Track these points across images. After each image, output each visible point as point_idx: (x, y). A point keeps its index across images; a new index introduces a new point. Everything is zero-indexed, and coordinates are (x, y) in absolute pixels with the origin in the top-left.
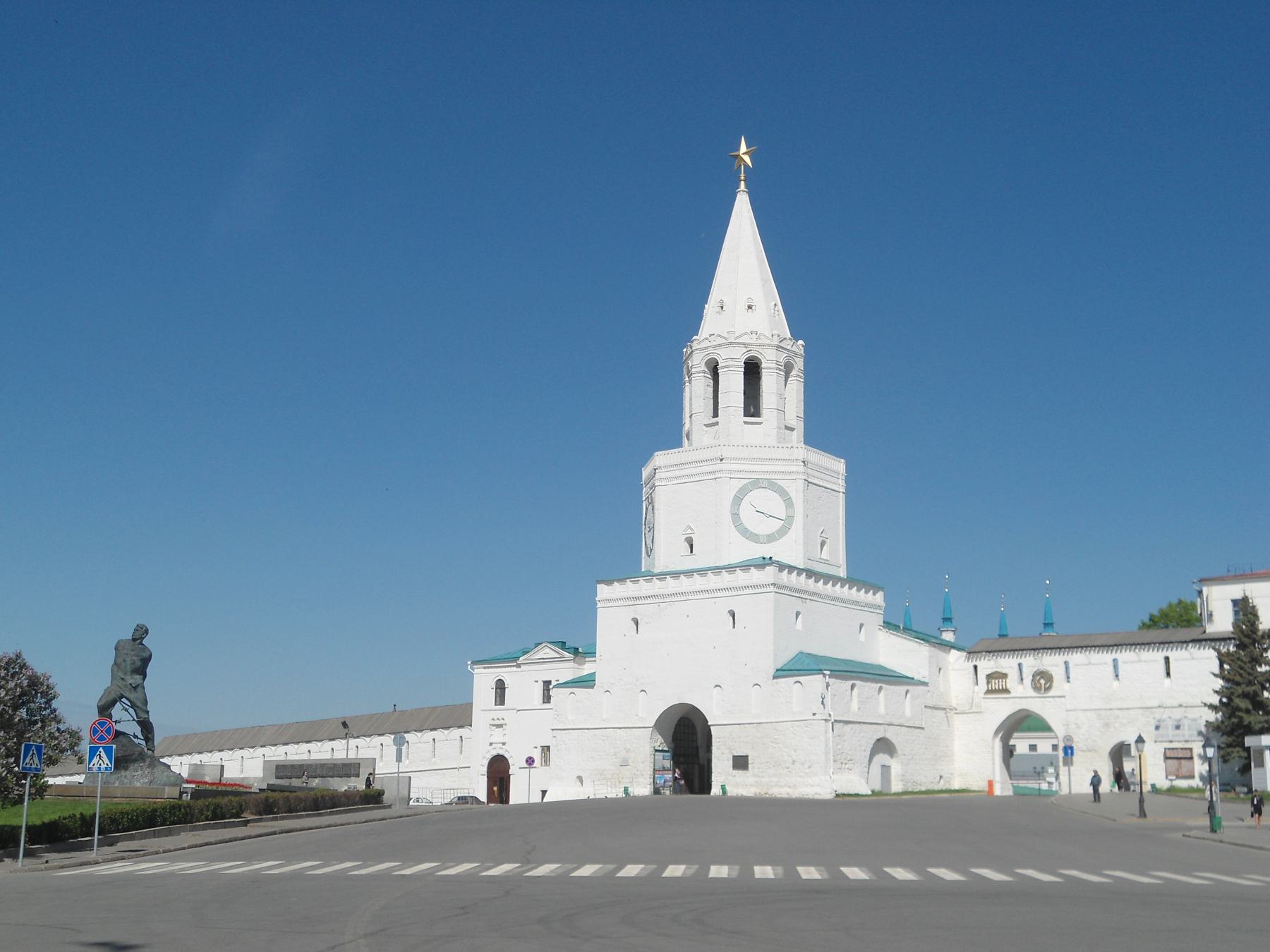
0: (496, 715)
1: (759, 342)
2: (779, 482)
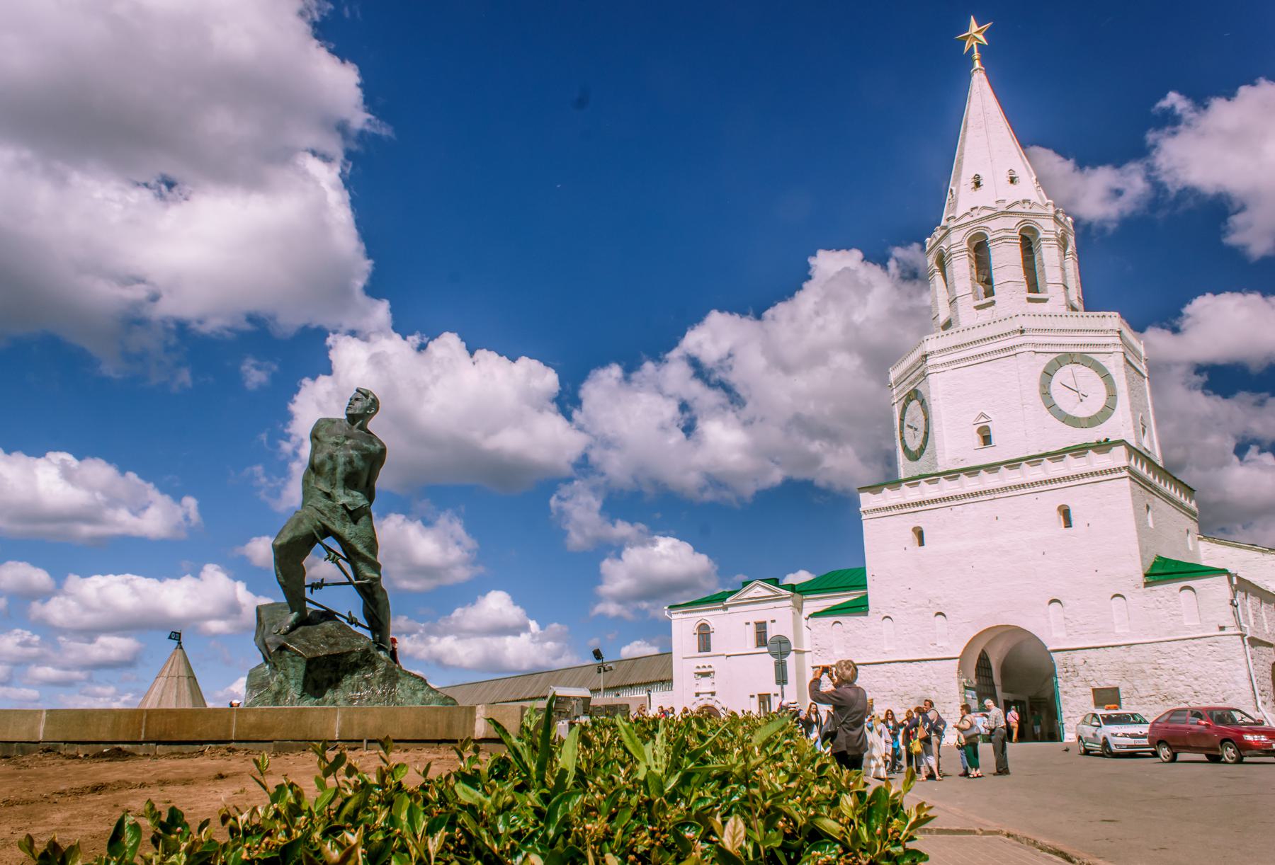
0: (700, 662)
1: (1033, 211)
2: (1093, 356)
